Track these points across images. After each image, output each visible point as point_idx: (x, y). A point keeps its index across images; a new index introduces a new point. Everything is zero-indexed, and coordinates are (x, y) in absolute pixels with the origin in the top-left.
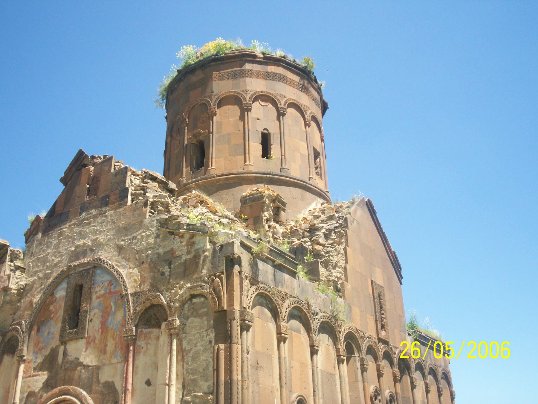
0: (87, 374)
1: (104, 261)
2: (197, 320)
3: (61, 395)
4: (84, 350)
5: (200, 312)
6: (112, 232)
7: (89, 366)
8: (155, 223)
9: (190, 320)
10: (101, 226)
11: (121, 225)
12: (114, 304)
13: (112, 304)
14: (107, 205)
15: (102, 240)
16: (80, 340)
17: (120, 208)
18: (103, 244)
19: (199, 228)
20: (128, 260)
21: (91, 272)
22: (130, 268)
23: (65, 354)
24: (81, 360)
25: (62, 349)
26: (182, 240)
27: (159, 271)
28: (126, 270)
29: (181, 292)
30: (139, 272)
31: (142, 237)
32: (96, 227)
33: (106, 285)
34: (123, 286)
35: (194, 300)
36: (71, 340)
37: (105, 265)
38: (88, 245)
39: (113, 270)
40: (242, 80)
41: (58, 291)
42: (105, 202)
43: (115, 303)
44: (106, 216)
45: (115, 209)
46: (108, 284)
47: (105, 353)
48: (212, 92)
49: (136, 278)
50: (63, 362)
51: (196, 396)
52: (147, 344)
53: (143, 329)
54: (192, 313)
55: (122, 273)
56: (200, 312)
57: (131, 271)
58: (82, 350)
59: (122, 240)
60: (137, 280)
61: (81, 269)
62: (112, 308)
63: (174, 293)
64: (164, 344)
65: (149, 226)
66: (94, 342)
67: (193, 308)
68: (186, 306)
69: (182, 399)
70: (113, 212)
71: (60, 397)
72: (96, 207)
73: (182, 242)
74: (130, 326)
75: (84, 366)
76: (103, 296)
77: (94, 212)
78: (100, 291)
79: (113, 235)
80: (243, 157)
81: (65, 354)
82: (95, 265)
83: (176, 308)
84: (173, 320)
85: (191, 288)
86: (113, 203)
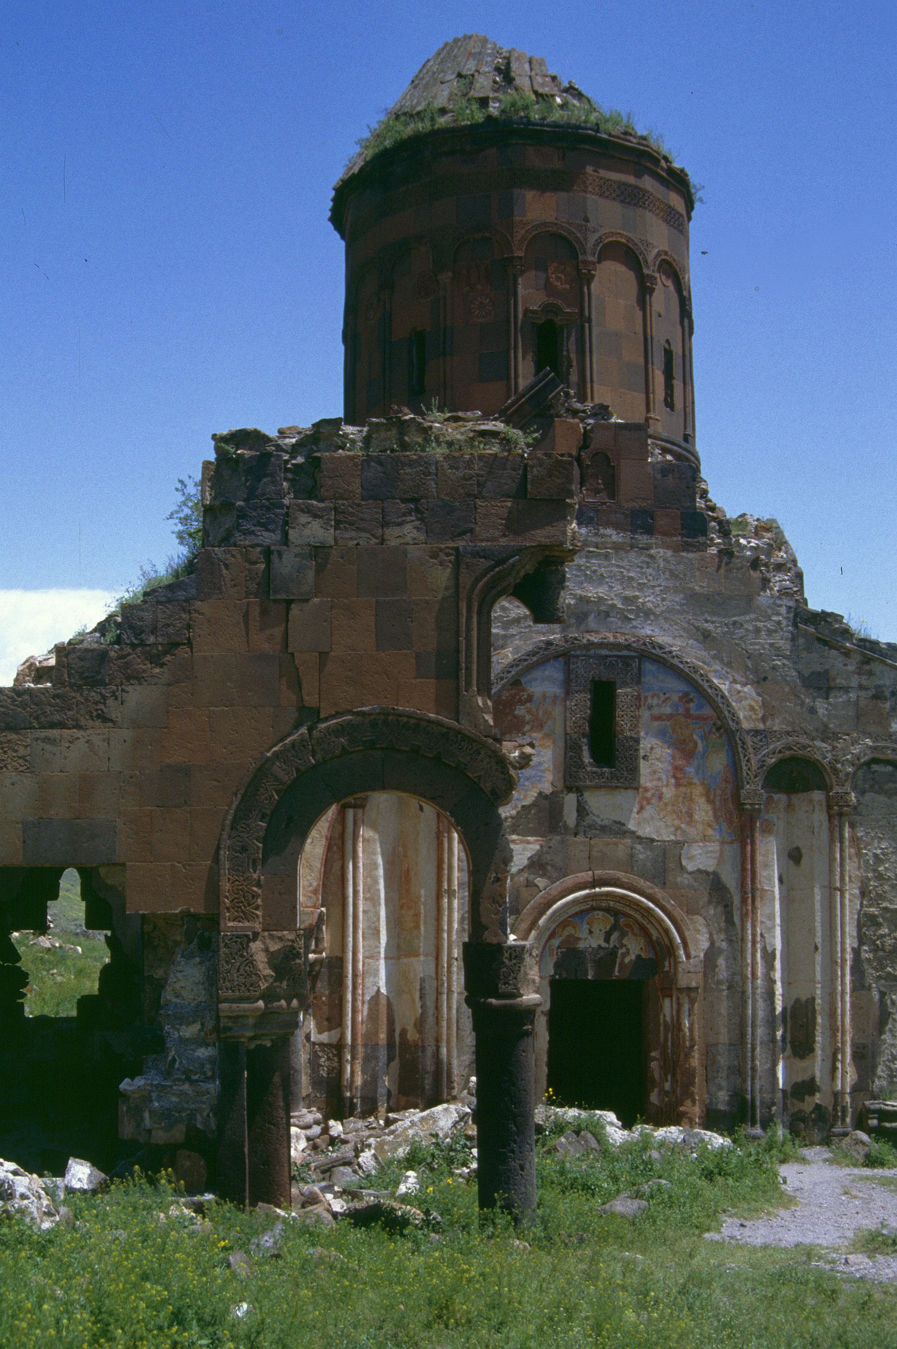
0: (648, 853)
1: (670, 652)
2: (882, 798)
3: (600, 886)
4: (635, 810)
5: (886, 787)
6: (678, 598)
7: (653, 840)
8: (783, 610)
9: (869, 796)
10: (642, 573)
11: (697, 588)
12: (702, 740)
13: (695, 737)
14: (649, 531)
15: (650, 605)
16: (622, 790)
17: (688, 551)
18: (654, 614)
19: (884, 651)
20: (729, 664)
21: (635, 665)
22: (735, 681)
23: (582, 810)
24: (631, 826)
25: (570, 800)
26: (848, 661)
27: (803, 704)
28: (727, 683)
29: (856, 750)
30: (758, 694)
31: (757, 630)
32: (628, 571)
33: (675, 697)
34: (726, 713)
35: (875, 767)
36: (598, 787)
37: (675, 661)
38: (613, 606)
39: (696, 677)
40: (640, 211)
41: (536, 680)
42: (641, 522)
43: (704, 738)
44: (651, 557)
45: (676, 550)
46: (681, 699)
47: (691, 821)
48: (587, 220)
49: (753, 703)
50: (578, 825)
51: (886, 909)
52: (778, 818)
53: (773, 795)
54: (872, 786)
55: (722, 687)
56: (886, 787)
57: (738, 687)
58: (631, 811)
59: (707, 621)
60: (757, 708)
61: (604, 652)
62: (696, 744)
63: (842, 749)
64: (820, 827)
65: (769, 611)
66: (660, 798)
67: (873, 779)
68: (860, 773)
69: (861, 910)
70: (669, 553)
71: (597, 889)
72: (618, 527)
73: (846, 665)
74: (753, 787)
75: (639, 837)
76: (670, 717)
77: (614, 536)
78: (658, 705)
79: (681, 605)
80: (643, 396)
81: (582, 810)
82: (645, 653)
83: (847, 774)
84: (846, 793)
85: (874, 749)
86: (665, 534)
